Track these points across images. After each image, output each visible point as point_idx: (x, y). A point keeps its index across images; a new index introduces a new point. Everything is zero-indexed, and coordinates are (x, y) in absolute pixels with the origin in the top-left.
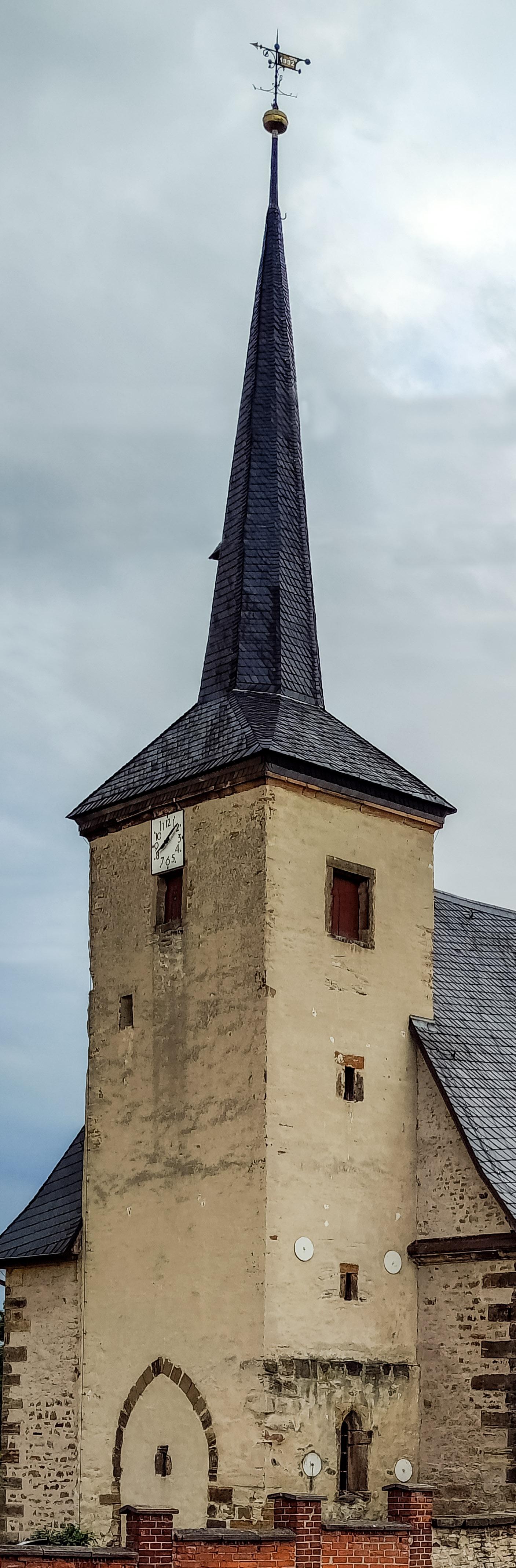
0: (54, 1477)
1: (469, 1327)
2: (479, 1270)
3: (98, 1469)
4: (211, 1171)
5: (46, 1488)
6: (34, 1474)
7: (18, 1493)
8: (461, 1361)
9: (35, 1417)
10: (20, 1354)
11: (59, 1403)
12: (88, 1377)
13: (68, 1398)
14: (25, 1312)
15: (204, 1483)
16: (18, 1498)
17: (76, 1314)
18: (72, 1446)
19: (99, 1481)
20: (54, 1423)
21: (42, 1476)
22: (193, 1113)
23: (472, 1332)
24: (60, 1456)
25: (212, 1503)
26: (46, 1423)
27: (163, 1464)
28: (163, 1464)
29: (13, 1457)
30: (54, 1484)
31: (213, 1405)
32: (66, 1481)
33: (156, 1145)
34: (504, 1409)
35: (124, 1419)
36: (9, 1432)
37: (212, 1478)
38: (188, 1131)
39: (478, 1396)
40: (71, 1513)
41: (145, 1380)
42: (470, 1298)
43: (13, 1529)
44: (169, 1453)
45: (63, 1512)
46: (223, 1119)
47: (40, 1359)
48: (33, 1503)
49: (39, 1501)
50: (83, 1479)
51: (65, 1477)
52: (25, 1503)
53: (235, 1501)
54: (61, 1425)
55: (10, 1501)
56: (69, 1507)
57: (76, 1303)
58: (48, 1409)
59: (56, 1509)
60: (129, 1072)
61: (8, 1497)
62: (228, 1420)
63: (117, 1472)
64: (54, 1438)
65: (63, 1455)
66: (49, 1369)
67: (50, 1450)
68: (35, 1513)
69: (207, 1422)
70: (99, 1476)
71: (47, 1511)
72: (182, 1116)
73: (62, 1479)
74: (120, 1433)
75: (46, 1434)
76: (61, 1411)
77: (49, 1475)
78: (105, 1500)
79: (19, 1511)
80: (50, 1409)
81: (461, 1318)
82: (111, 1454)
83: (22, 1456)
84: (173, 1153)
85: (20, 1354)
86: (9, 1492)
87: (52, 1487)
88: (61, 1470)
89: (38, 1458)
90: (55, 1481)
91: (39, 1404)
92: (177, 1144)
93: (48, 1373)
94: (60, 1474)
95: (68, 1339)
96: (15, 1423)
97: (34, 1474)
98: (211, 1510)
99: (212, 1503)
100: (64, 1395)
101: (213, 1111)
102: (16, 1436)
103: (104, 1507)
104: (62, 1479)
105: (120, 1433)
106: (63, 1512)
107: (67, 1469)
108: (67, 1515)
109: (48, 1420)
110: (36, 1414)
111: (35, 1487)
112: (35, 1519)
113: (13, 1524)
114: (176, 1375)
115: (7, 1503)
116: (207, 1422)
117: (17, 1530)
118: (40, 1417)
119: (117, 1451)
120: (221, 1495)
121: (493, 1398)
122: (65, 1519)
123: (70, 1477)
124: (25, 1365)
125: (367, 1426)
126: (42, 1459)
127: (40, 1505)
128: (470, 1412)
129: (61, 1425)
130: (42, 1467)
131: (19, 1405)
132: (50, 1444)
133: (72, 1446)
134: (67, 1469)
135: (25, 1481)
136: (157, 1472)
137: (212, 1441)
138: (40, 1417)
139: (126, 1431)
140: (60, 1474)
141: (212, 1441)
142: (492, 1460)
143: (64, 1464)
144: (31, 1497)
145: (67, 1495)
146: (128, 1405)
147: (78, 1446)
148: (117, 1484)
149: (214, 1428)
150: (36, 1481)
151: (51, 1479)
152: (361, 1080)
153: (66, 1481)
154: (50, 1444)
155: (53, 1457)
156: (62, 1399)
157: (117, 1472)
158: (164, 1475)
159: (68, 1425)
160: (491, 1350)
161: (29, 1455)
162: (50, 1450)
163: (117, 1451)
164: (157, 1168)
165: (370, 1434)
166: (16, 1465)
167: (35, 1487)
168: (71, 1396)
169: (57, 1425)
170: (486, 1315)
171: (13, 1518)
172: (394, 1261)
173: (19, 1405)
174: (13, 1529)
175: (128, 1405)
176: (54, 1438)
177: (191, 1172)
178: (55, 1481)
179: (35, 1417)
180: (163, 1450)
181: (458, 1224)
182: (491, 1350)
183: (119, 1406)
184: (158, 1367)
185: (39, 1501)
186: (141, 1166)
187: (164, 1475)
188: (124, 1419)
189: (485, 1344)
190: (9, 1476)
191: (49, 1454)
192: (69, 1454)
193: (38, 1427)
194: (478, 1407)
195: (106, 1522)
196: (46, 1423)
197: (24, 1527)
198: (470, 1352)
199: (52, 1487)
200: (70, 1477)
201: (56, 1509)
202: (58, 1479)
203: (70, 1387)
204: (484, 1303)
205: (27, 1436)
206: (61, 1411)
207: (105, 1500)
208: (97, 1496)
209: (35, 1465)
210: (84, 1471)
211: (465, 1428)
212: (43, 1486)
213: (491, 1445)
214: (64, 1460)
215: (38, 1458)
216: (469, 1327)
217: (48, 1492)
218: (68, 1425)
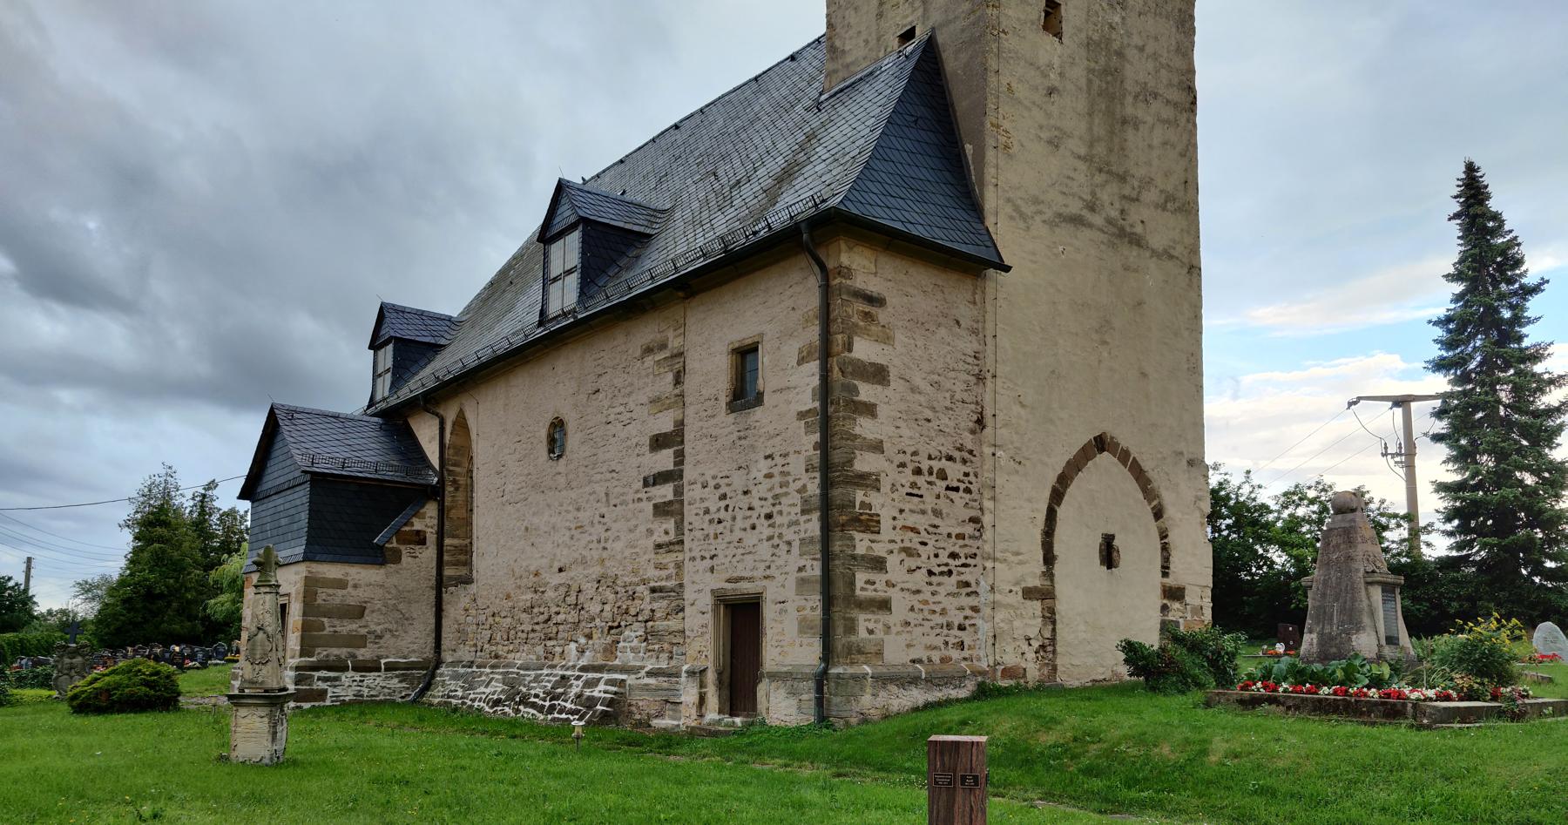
0: (943, 558)
3: (1018, 554)
5: (930, 573)
6: (909, 552)
9: (908, 471)
10: (878, 374)
11: (950, 458)
13: (966, 455)
14: (882, 315)
16: (880, 586)
17: (976, 346)
18: (973, 520)
19: (1020, 570)
20: (944, 484)
21: (924, 557)
26: (930, 483)
27: (1109, 555)
28: (1109, 555)
29: (870, 524)
32: (964, 565)
35: (1057, 496)
36: (858, 485)
37: (1165, 575)
40: (975, 609)
43: (871, 632)
44: (1116, 543)
45: (962, 608)
47: (914, 390)
48: (907, 595)
49: (918, 592)
50: (997, 565)
51: (963, 560)
52: (895, 595)
53: (1187, 599)
54: (957, 489)
55: (862, 589)
56: (972, 601)
57: (975, 332)
58: (932, 463)
59: (950, 604)
61: (859, 583)
62: (1179, 515)
63: (1049, 559)
64: (943, 504)
65: (958, 530)
66: (933, 409)
67: (937, 521)
69: (1158, 514)
70: (1021, 563)
71: (933, 607)
73: (958, 562)
75: (929, 500)
76: (955, 471)
77: (936, 556)
78: (1029, 593)
79: (884, 605)
80: (936, 465)
83: (886, 524)
85: (878, 374)
86: (861, 577)
87: (942, 573)
88: (957, 549)
89: (914, 530)
91: (915, 453)
94: (953, 556)
96: (870, 474)
97: (909, 552)
98: (1164, 608)
100: (959, 450)
102: (873, 494)
103: (1028, 603)
104: (958, 562)
106: (962, 608)
107: (967, 550)
108: (968, 612)
109: (933, 478)
110: (911, 467)
111: (910, 571)
113: (871, 626)
115: (858, 592)
116: (1158, 514)
117: (879, 635)
118: (918, 472)
123: (969, 561)
124: (889, 391)
126: (923, 533)
127: (920, 597)
129: (957, 489)
130: (924, 544)
131: (878, 447)
132: (937, 513)
133: (973, 520)
134: (967, 550)
135: (892, 561)
136: (1102, 563)
137: (1163, 535)
139: (1061, 512)
140: (953, 556)
141: (1163, 535)
143: (961, 542)
144: (905, 586)
145: (967, 584)
146: (1064, 481)
148: (1049, 575)
149: (1166, 521)
150: (912, 563)
151: (938, 561)
153: (964, 565)
154: (937, 513)
155: (944, 530)
156: (957, 454)
157: (1049, 559)
158: (1109, 567)
161: (899, 523)
162: (937, 521)
166: (873, 537)
167: (910, 571)
168: (971, 452)
169: (948, 488)
171: (869, 616)
173: (878, 447)
174: (871, 632)
175: (1064, 481)
176: (943, 504)
179: (908, 471)
183: (1051, 479)
184: (1101, 444)
185: (918, 592)
187: (1109, 567)
188: (1057, 496)
192: (969, 529)
193: (914, 485)
195: (1033, 622)
196: (930, 483)
197: (894, 630)
199: (942, 573)
200: (969, 561)
201: (950, 604)
202: (951, 561)
203: (968, 441)
205: (895, 495)
206: (955, 471)
207: (1029, 593)
208: (1018, 589)
209: (912, 541)
210: (998, 555)
212: (924, 571)
214: (960, 536)
215: (914, 530)
217: (934, 579)
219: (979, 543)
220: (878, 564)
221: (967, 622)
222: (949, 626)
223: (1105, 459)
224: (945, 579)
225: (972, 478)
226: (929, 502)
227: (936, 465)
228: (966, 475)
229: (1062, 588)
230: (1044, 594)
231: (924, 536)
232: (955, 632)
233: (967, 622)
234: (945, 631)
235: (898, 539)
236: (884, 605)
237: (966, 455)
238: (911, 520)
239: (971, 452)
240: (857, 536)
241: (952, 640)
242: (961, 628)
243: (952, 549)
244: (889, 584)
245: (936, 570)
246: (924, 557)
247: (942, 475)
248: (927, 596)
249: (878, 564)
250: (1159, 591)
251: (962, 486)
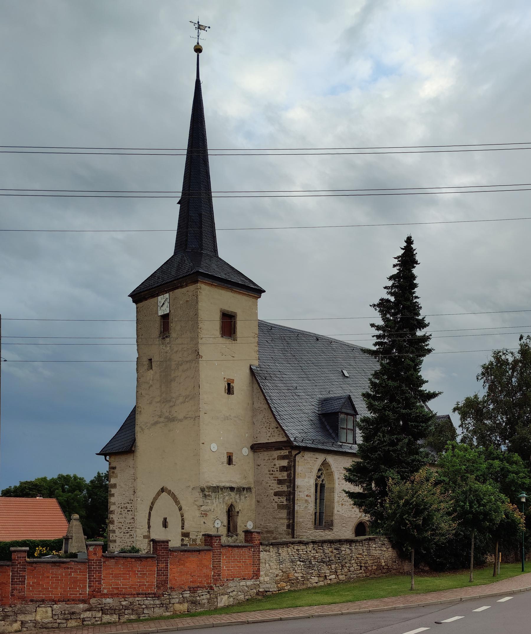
0: (127, 528)
1: (272, 474)
2: (276, 454)
4: (181, 420)
6: (120, 528)
7: (114, 535)
8: (270, 486)
10: (114, 486)
11: (128, 503)
12: (138, 493)
14: (116, 471)
15: (180, 530)
17: (134, 471)
18: (133, 518)
22: (174, 400)
23: (274, 476)
27: (165, 524)
28: (165, 524)
29: (112, 522)
31: (183, 503)
33: (161, 412)
34: (285, 503)
35: (151, 508)
37: (183, 529)
38: (171, 407)
39: (276, 498)
40: (133, 542)
41: (158, 494)
42: (273, 464)
46: (184, 402)
47: (121, 487)
52: (117, 539)
53: (191, 537)
56: (132, 540)
59: (128, 540)
60: (151, 386)
62: (188, 508)
63: (149, 527)
67: (125, 520)
69: (180, 509)
72: (170, 401)
74: (150, 513)
75: (124, 514)
76: (129, 506)
78: (145, 537)
79: (115, 541)
80: (125, 505)
81: (269, 471)
82: (147, 521)
84: (167, 414)
85: (114, 486)
86: (111, 535)
89: (121, 523)
92: (168, 411)
93: (124, 493)
94: (129, 528)
95: (131, 481)
97: (120, 528)
98: (182, 540)
101: (181, 399)
105: (150, 513)
112: (120, 544)
114: (169, 492)
116: (180, 509)
118: (122, 508)
119: (149, 520)
120: (186, 535)
121: (281, 499)
124: (116, 490)
125: (237, 510)
128: (273, 504)
131: (114, 504)
132: (125, 518)
133: (133, 518)
135: (117, 531)
136: (163, 527)
137: (182, 516)
138: (122, 508)
139: (152, 513)
140: (129, 528)
141: (182, 516)
142: (282, 521)
146: (153, 504)
147: (135, 518)
148: (149, 531)
149: (183, 511)
150: (120, 531)
152: (233, 387)
154: (125, 518)
155: (127, 522)
156: (129, 502)
157: (149, 527)
159: (132, 511)
160: (280, 482)
162: (125, 520)
163: (149, 520)
164: (162, 420)
165: (238, 512)
170: (278, 470)
172: (246, 451)
173: (114, 504)
175: (153, 504)
177: (174, 421)
180: (165, 519)
181: (268, 438)
182: (280, 482)
183: (149, 504)
184: (163, 490)
186: (156, 419)
188: (151, 508)
189: (278, 480)
190: (111, 529)
192: (132, 521)
193: (121, 511)
194: (276, 502)
198: (273, 483)
201: (128, 540)
204: (278, 466)
207: (145, 537)
210: (137, 527)
211: (272, 510)
213: (281, 515)
215: (121, 523)
216: (272, 474)
218: (132, 511)
220: (114, 532)
224: (127, 534)
226: (124, 515)
227: (125, 505)
238: (120, 520)
240: (111, 525)
244: (116, 536)
248: (123, 539)
250: (180, 534)
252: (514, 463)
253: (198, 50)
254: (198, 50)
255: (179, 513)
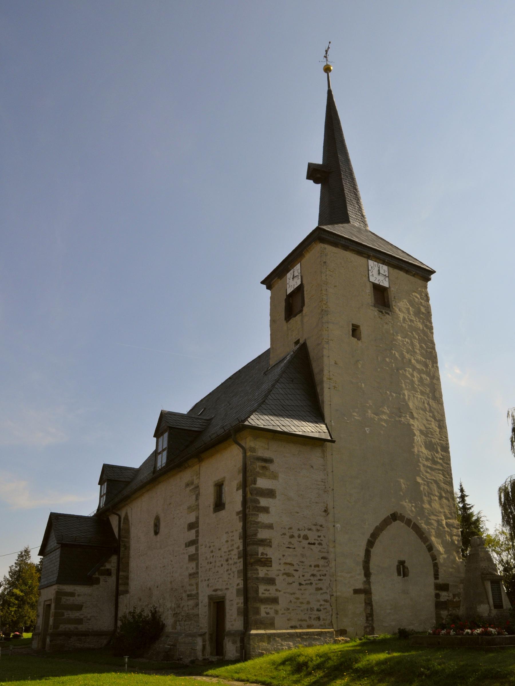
0: (308, 576)
5: (300, 584)
6: (288, 575)
10: (270, 493)
11: (310, 530)
13: (319, 528)
14: (272, 467)
15: (431, 580)
21: (297, 577)
24: (313, 564)
25: (437, 592)
29: (267, 562)
30: (309, 582)
32: (320, 580)
35: (371, 544)
36: (260, 545)
44: (406, 564)
49: (294, 594)
51: (319, 577)
54: (314, 544)
55: (263, 593)
58: (300, 532)
63: (367, 574)
65: (316, 563)
68: (291, 601)
73: (316, 578)
80: (302, 533)
85: (270, 493)
86: (262, 588)
87: (306, 584)
88: (315, 572)
90: (310, 580)
94: (313, 575)
96: (266, 540)
97: (288, 575)
98: (437, 596)
99: (437, 592)
100: (315, 525)
107: (320, 573)
110: (288, 535)
115: (260, 595)
118: (292, 537)
120: (441, 587)
122: (321, 605)
123: (322, 577)
129: (314, 544)
130: (297, 570)
134: (320, 573)
136: (399, 574)
139: (375, 551)
140: (313, 575)
143: (317, 569)
148: (368, 582)
150: (290, 580)
151: (305, 578)
153: (320, 580)
154: (303, 555)
156: (314, 528)
157: (367, 574)
159: (320, 544)
161: (283, 561)
166: (269, 568)
171: (267, 606)
173: (270, 527)
174: (267, 613)
178: (310, 580)
183: (368, 536)
184: (394, 517)
191: (302, 562)
192: (321, 562)
197: (280, 612)
199: (306, 584)
200: (322, 577)
202: (312, 578)
203: (321, 520)
207: (356, 592)
209: (291, 569)
217: (302, 587)
219: (328, 569)
220: (271, 581)
221: (322, 608)
222: (312, 609)
223: (397, 524)
224: (309, 587)
225: (322, 538)
228: (319, 537)
229: (374, 588)
230: (366, 592)
231: (296, 567)
232: (315, 612)
233: (322, 608)
234: (309, 612)
235: (282, 569)
236: (275, 601)
237: (319, 528)
238: (289, 560)
239: (321, 526)
240: (260, 568)
241: (313, 617)
242: (318, 610)
243: (312, 573)
245: (303, 583)
246: (297, 577)
247: (306, 538)
249: (271, 581)
250: (433, 587)
251: (317, 542)
252: (449, 492)
253: (327, 70)
254: (327, 70)
255: (428, 554)
